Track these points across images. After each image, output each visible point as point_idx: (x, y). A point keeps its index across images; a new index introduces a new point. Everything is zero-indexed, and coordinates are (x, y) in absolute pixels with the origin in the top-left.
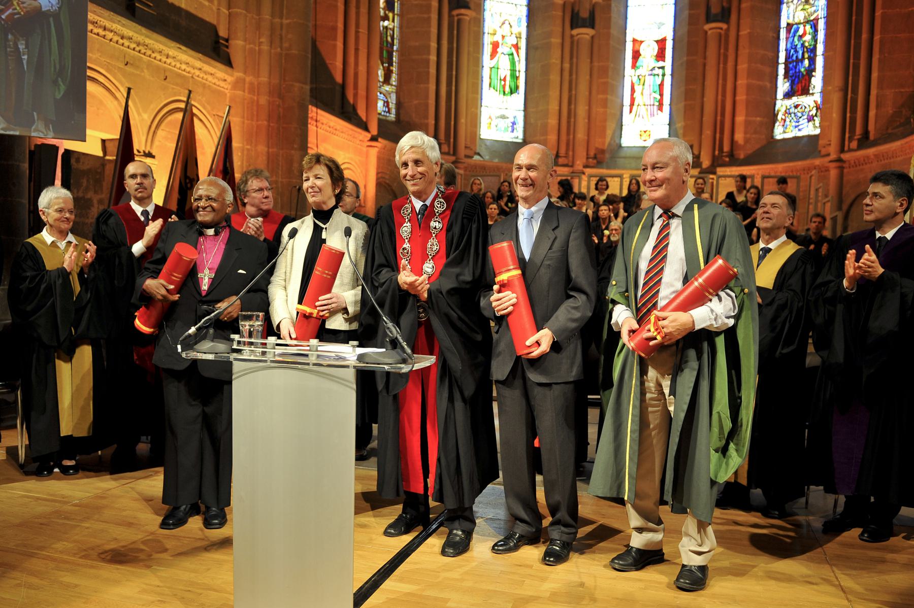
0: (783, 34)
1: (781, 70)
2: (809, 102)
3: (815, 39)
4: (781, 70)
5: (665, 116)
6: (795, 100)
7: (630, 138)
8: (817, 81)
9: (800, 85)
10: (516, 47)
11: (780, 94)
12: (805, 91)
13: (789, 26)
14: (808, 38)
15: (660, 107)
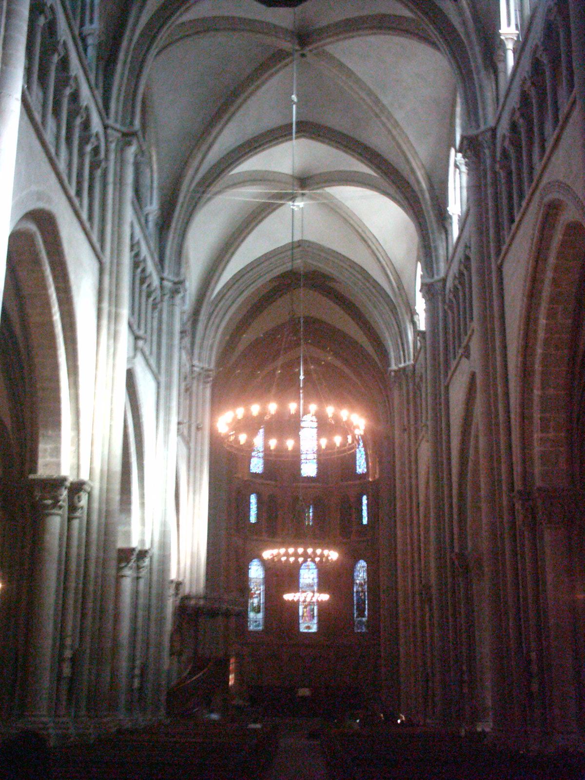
0: (355, 595)
1: (355, 607)
2: (364, 619)
3: (365, 597)
4: (355, 607)
5: (315, 621)
6: (359, 619)
7: (303, 629)
8: (366, 613)
9: (362, 614)
10: (260, 594)
11: (355, 616)
12: (364, 616)
13: (357, 592)
14: (363, 597)
15: (313, 617)
